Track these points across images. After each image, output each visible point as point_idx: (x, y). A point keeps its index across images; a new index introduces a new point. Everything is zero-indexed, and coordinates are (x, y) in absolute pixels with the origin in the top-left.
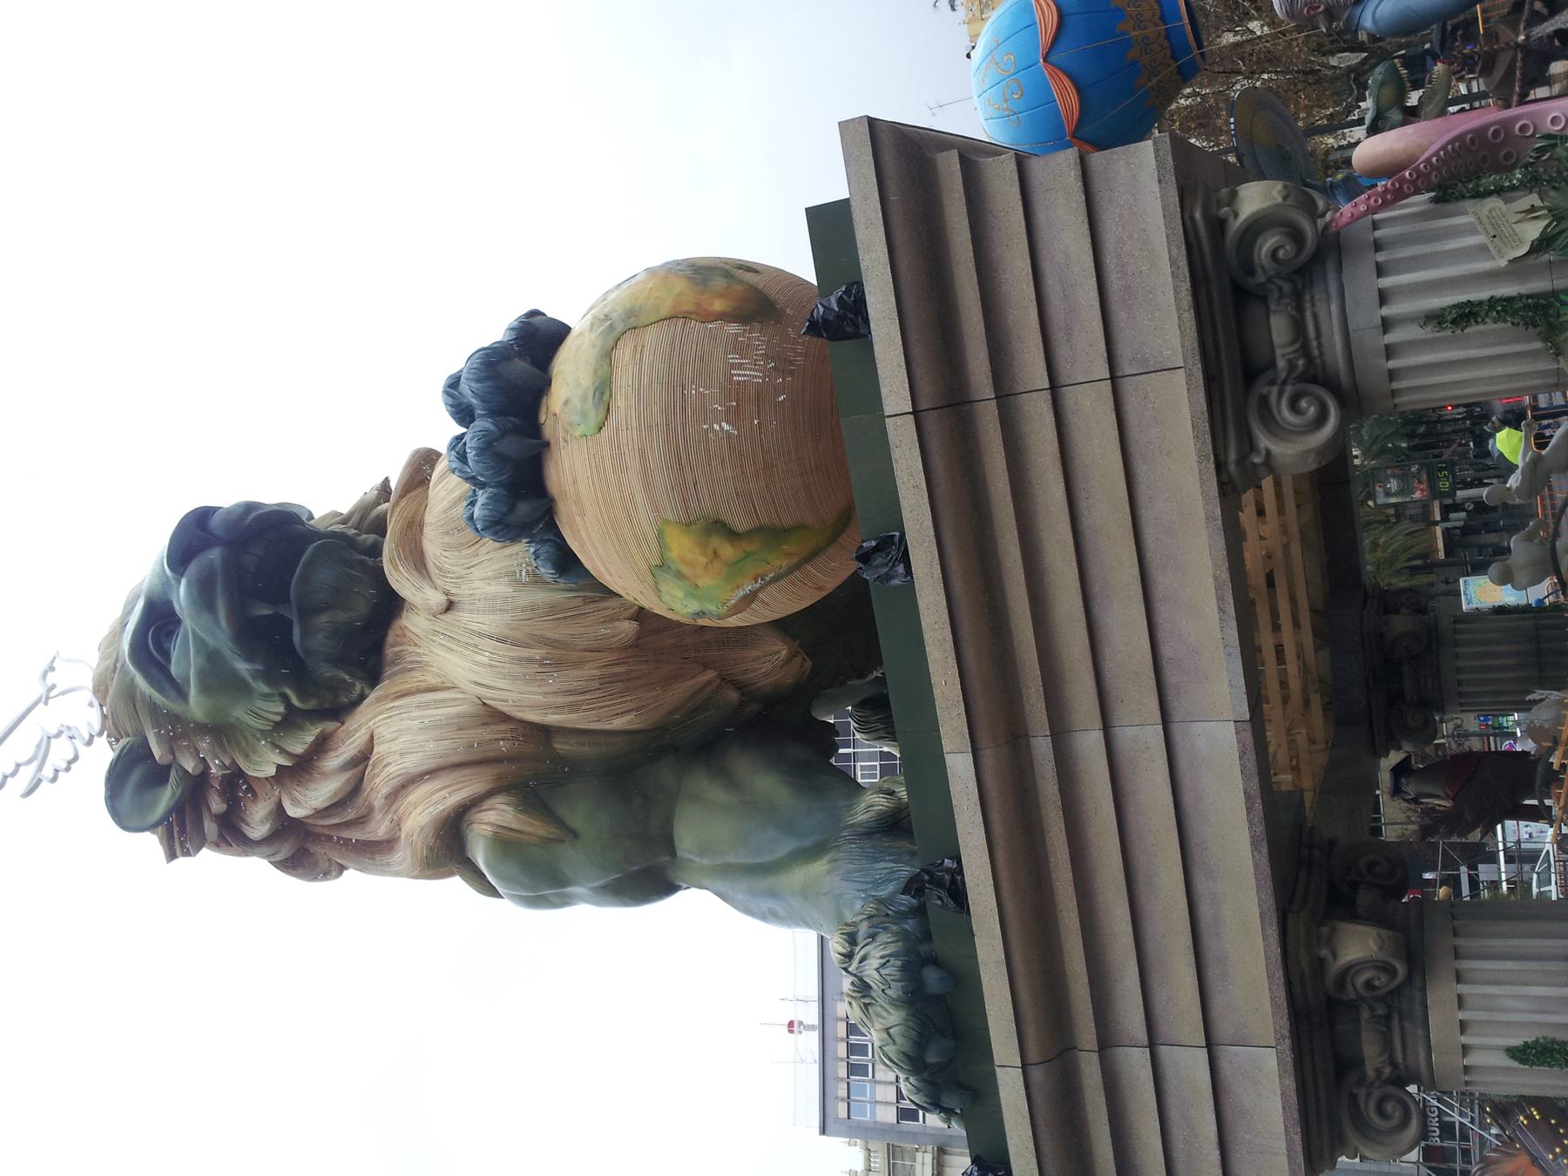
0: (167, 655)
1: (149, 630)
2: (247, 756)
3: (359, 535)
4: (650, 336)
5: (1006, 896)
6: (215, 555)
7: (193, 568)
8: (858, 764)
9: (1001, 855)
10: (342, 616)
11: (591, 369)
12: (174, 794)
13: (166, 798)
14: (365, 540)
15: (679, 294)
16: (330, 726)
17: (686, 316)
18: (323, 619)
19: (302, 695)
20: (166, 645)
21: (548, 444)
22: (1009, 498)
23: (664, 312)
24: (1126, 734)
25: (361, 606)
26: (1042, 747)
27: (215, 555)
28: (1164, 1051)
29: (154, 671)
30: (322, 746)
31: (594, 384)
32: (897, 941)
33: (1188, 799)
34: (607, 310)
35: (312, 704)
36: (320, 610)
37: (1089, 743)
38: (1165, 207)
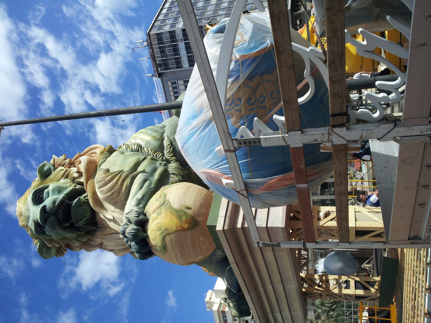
0: (44, 231)
1: (38, 227)
2: (70, 242)
3: (76, 186)
4: (173, 236)
5: (256, 307)
6: (52, 219)
7: (48, 223)
8: (166, 49)
9: (255, 303)
10: (85, 219)
11: (160, 242)
12: (55, 250)
13: (54, 251)
14: (79, 188)
15: (176, 224)
16: (90, 237)
17: (180, 230)
18: (81, 221)
19: (80, 231)
20: (43, 229)
21: (151, 248)
22: (254, 266)
23: (174, 229)
24: (276, 286)
25: (88, 215)
26: (261, 290)
27: (52, 219)
28: (282, 313)
30: (89, 240)
31: (162, 245)
32: (234, 302)
33: (287, 291)
34: (159, 225)
35: (83, 233)
36: (80, 220)
37: (269, 288)
38: (284, 235)
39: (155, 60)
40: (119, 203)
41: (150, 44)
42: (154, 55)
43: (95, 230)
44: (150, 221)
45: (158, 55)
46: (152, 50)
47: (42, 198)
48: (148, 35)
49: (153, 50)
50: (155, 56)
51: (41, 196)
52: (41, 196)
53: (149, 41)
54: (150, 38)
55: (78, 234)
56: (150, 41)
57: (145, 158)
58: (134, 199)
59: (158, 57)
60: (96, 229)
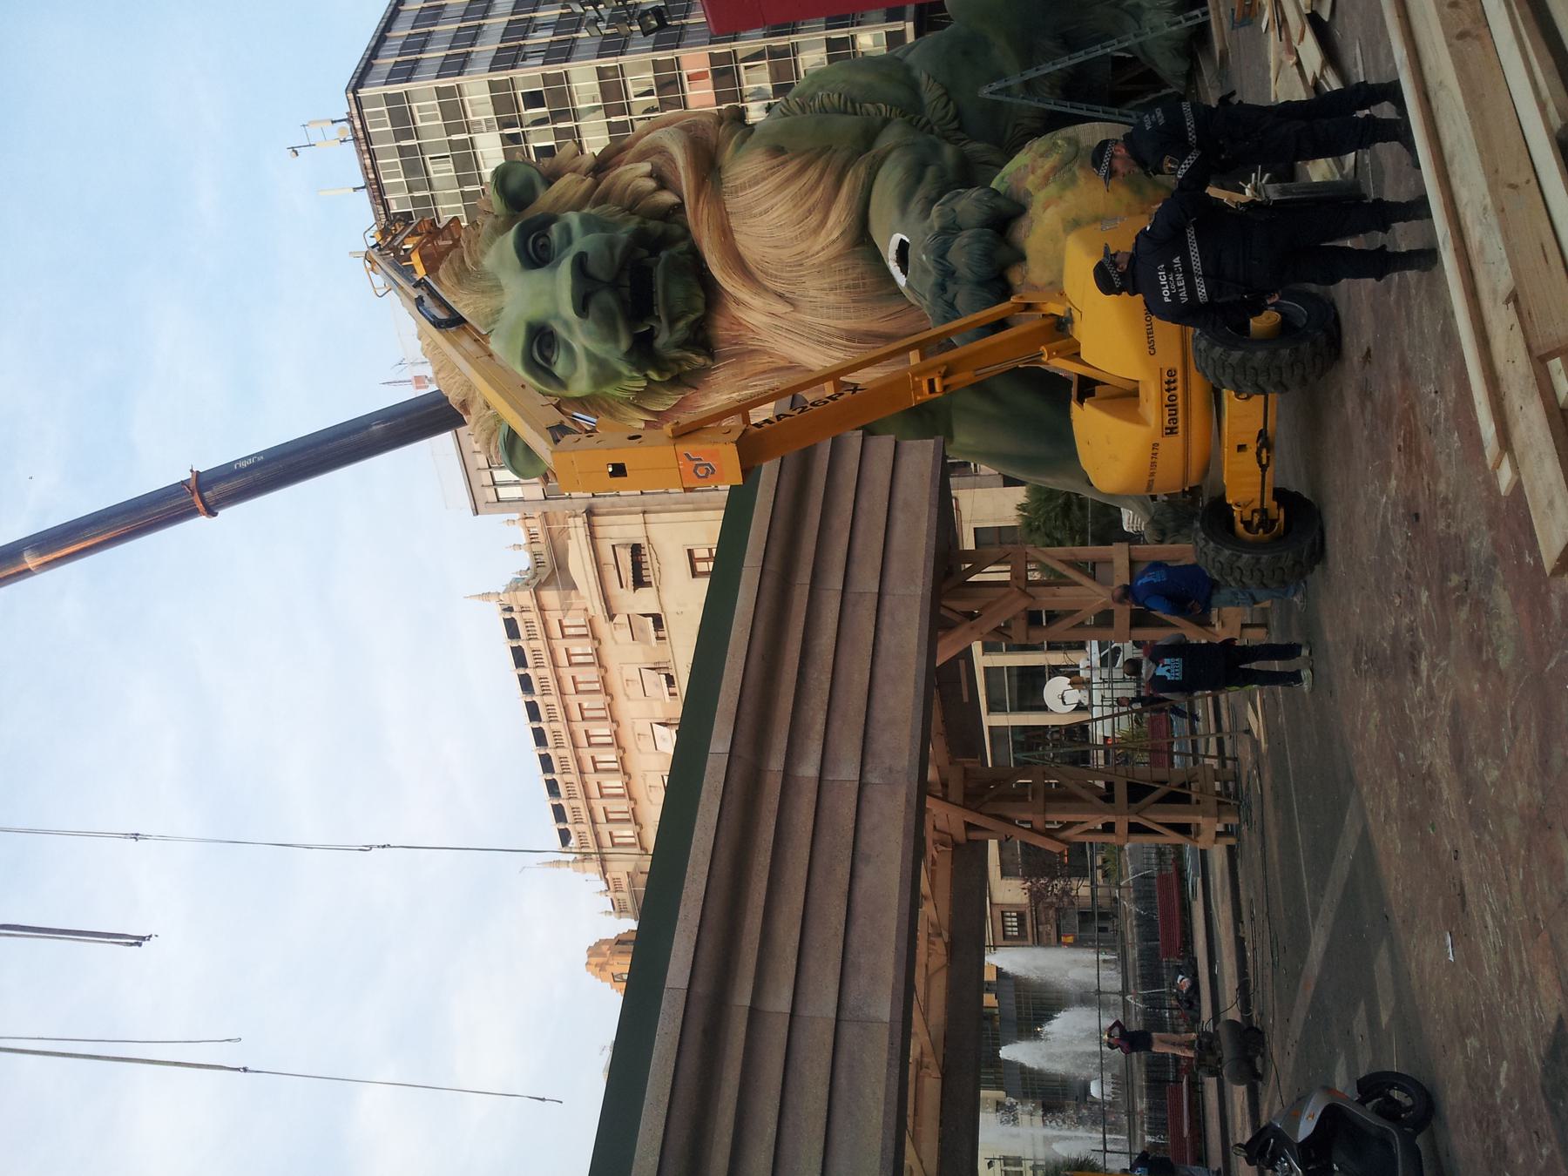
0: (547, 360)
19: (660, 372)
20: (547, 353)
29: (540, 373)
39: (382, 199)
40: (818, 253)
41: (361, 134)
42: (377, 180)
43: (706, 370)
44: (1035, 210)
45: (394, 178)
46: (371, 158)
47: (546, 247)
48: (353, 102)
49: (373, 157)
50: (384, 182)
51: (541, 242)
52: (541, 242)
53: (358, 124)
54: (359, 113)
55: (650, 381)
56: (362, 124)
57: (886, 122)
58: (916, 199)
59: (397, 187)
60: (709, 363)
